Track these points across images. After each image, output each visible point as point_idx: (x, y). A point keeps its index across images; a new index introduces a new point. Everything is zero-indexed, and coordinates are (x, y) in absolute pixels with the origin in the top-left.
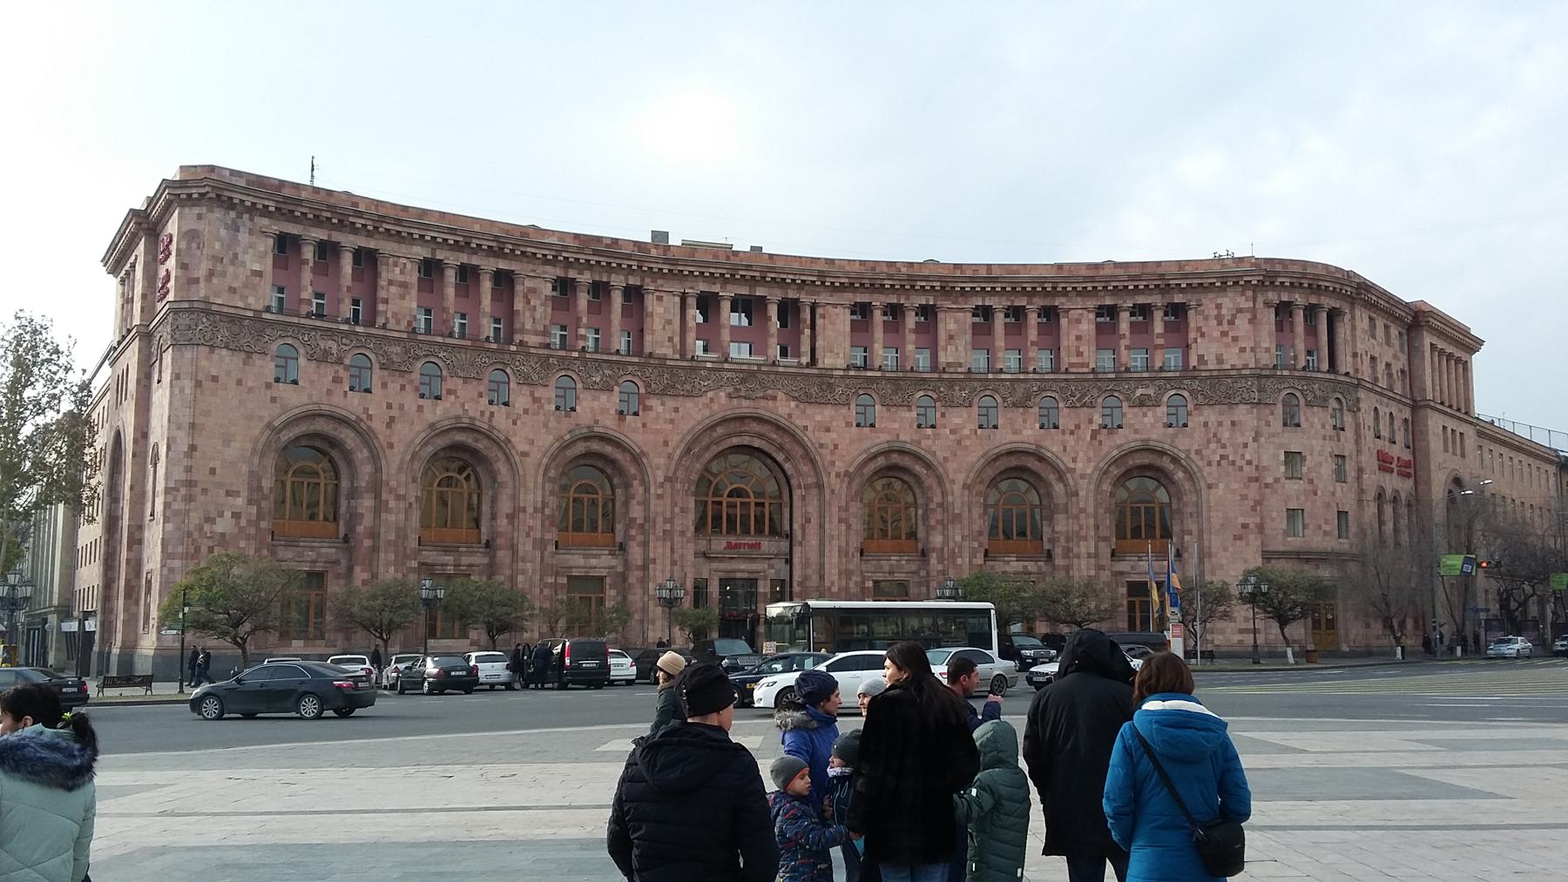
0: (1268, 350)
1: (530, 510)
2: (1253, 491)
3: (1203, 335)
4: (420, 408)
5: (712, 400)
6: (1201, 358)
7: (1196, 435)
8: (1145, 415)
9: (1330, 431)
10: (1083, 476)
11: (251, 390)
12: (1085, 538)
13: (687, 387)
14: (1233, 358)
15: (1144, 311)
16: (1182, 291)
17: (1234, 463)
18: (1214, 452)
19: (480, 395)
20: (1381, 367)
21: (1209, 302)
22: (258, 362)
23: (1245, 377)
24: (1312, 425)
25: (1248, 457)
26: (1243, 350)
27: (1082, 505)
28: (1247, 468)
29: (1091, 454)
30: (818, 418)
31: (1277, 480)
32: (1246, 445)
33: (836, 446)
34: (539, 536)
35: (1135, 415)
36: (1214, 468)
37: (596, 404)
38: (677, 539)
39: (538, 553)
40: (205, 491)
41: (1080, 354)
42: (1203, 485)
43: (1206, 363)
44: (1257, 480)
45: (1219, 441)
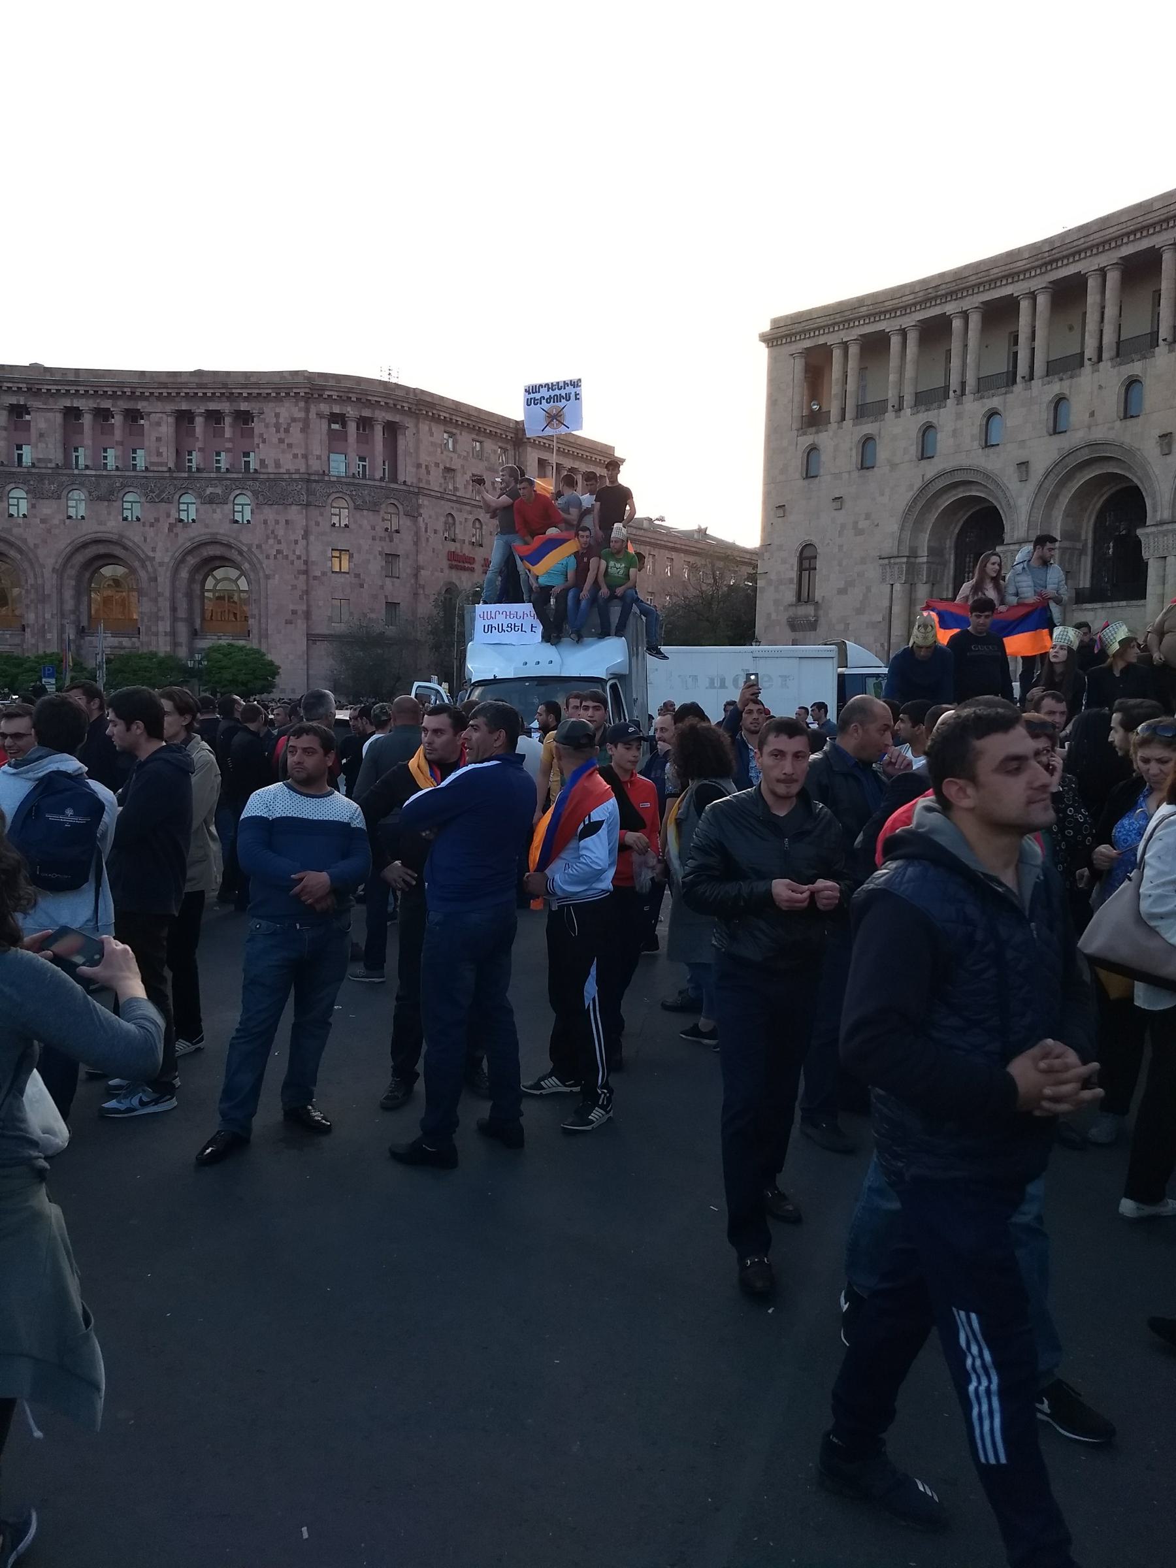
0: (319, 458)
3: (264, 441)
6: (262, 462)
8: (214, 511)
10: (161, 564)
12: (162, 619)
14: (288, 464)
15: (214, 417)
16: (246, 399)
17: (287, 557)
18: (272, 547)
21: (269, 409)
23: (295, 480)
24: (361, 526)
25: (298, 553)
26: (295, 456)
28: (297, 562)
32: (296, 542)
36: (272, 561)
41: (159, 454)
42: (261, 574)
43: (266, 467)
45: (276, 537)
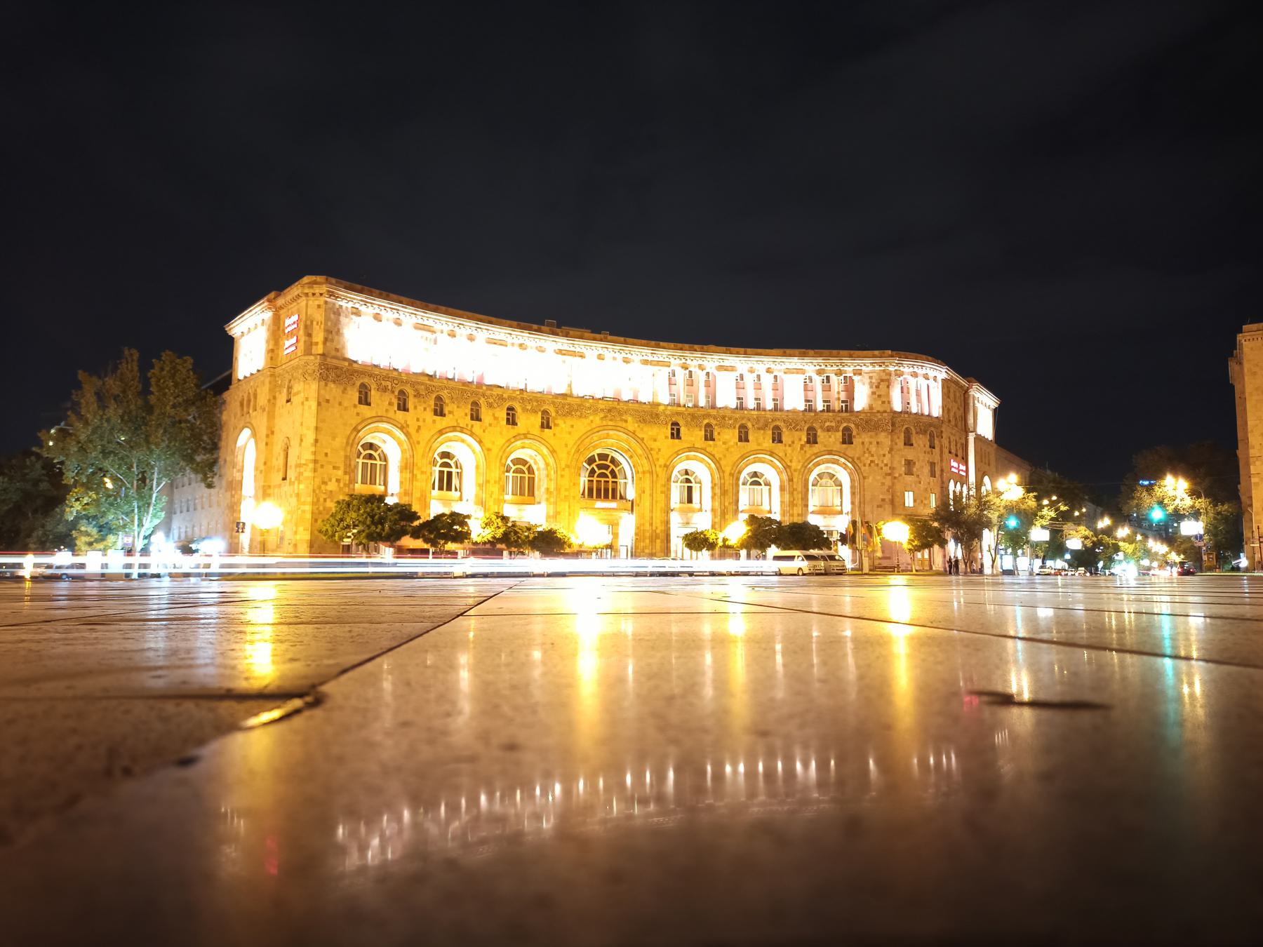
2: (888, 481)
4: (434, 422)
11: (346, 408)
20: (952, 414)
40: (322, 466)
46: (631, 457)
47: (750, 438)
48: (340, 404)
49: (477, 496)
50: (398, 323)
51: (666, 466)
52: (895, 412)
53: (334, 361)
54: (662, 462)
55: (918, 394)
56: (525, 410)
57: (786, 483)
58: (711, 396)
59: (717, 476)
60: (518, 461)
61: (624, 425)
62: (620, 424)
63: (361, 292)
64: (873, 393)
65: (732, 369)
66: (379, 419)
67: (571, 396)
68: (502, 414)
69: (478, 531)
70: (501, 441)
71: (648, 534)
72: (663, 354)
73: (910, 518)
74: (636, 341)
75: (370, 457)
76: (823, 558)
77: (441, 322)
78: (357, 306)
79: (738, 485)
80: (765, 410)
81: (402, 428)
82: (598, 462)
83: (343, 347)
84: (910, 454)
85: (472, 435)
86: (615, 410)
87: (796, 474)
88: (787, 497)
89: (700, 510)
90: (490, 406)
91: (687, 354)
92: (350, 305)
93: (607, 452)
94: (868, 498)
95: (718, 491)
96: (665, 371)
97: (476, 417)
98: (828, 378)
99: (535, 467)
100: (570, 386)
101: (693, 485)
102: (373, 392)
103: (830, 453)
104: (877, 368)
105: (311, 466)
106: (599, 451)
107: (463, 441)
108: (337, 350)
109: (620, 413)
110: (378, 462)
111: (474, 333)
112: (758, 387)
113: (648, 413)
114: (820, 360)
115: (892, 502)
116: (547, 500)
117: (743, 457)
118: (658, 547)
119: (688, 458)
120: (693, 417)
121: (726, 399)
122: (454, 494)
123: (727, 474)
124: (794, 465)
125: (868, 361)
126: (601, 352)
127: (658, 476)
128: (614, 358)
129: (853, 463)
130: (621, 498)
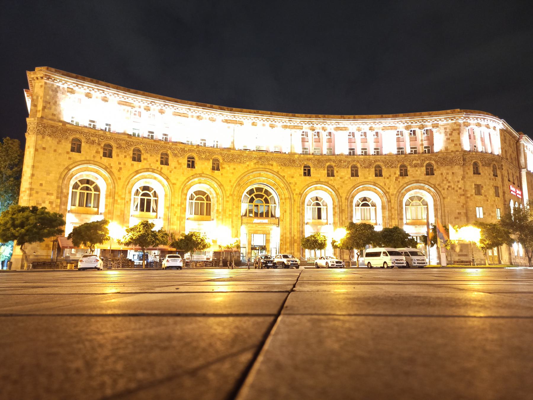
1: (176, 205)
2: (462, 200)
4: (132, 165)
5: (248, 165)
7: (438, 178)
8: (417, 171)
9: (493, 177)
10: (392, 195)
11: (60, 154)
13: (239, 160)
17: (454, 189)
18: (445, 184)
19: (157, 161)
20: (508, 155)
22: (64, 144)
24: (485, 174)
25: (459, 186)
27: (392, 206)
28: (459, 191)
29: (396, 186)
30: (289, 173)
31: (472, 195)
32: (458, 182)
33: (296, 184)
34: (179, 215)
35: (413, 171)
37: (203, 166)
38: (234, 218)
39: (179, 222)
40: (37, 193)
44: (463, 195)
45: (447, 180)
46: (277, 189)
47: (359, 174)
48: (55, 151)
49: (165, 215)
50: (105, 100)
51: (301, 194)
52: (465, 151)
53: (50, 122)
54: (297, 191)
55: (482, 140)
56: (200, 158)
57: (386, 204)
58: (331, 149)
59: (336, 200)
60: (197, 193)
61: (271, 167)
62: (268, 167)
63: (76, 78)
64: (448, 139)
65: (345, 129)
66: (88, 162)
67: (234, 149)
68: (185, 161)
69: (117, 236)
70: (183, 178)
71: (288, 240)
72: (297, 121)
73: (480, 224)
74: (279, 113)
75: (87, 189)
76: (406, 254)
77: (139, 101)
78: (71, 87)
79: (351, 206)
80: (369, 155)
81: (106, 168)
82: (256, 193)
83: (60, 113)
84: (478, 180)
85: (161, 174)
86: (263, 158)
87: (393, 197)
88: (387, 213)
89: (327, 224)
90: (175, 155)
91: (314, 120)
92: (66, 86)
93: (261, 186)
94: (447, 209)
95: (337, 210)
96: (300, 132)
97: (165, 161)
98: (414, 132)
99: (211, 196)
100: (233, 143)
101: (322, 207)
102: (83, 144)
103: (417, 182)
104: (450, 122)
105: (28, 192)
106: (257, 186)
107: (155, 178)
108: (54, 115)
109: (268, 160)
110: (93, 192)
111: (164, 108)
112: (365, 141)
113: (288, 160)
114: (407, 119)
115: (466, 214)
116: (217, 217)
117: (354, 187)
118: (296, 249)
119: (316, 189)
120: (319, 161)
121: (342, 148)
122: (151, 214)
123: (343, 199)
124: (391, 191)
125: (442, 117)
126: (254, 121)
127: (296, 201)
128: (264, 125)
129: (435, 187)
130: (272, 216)
